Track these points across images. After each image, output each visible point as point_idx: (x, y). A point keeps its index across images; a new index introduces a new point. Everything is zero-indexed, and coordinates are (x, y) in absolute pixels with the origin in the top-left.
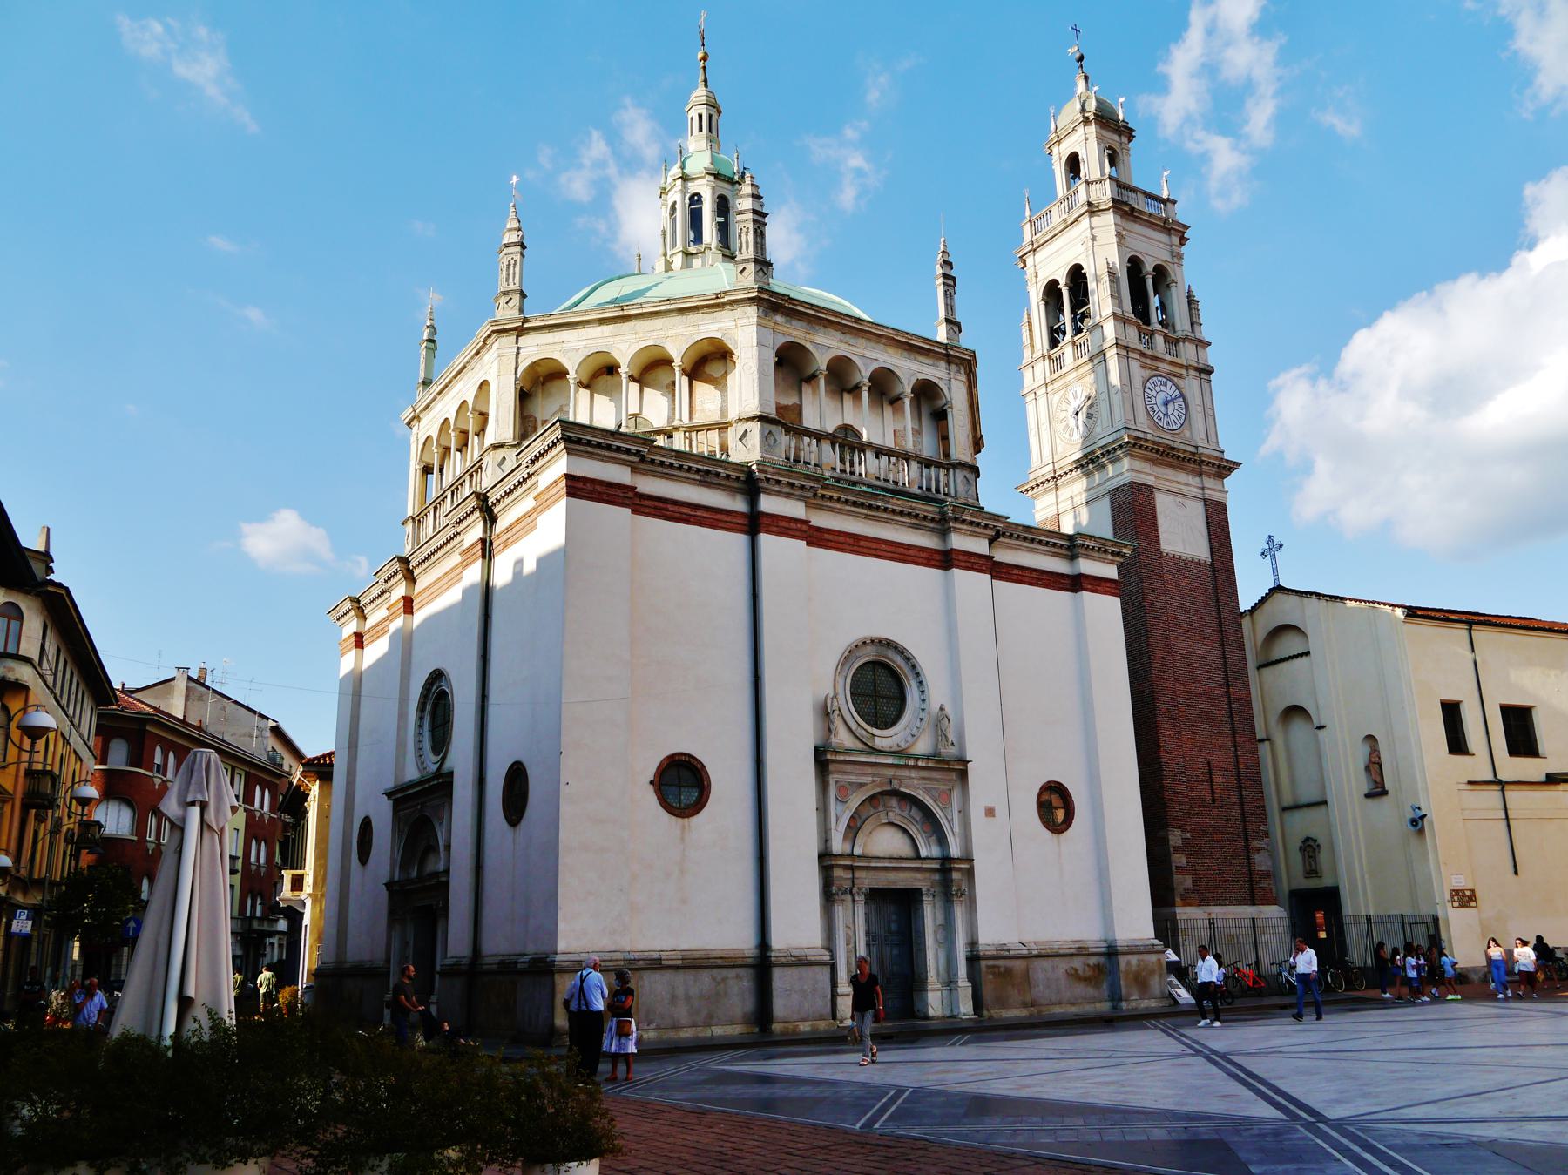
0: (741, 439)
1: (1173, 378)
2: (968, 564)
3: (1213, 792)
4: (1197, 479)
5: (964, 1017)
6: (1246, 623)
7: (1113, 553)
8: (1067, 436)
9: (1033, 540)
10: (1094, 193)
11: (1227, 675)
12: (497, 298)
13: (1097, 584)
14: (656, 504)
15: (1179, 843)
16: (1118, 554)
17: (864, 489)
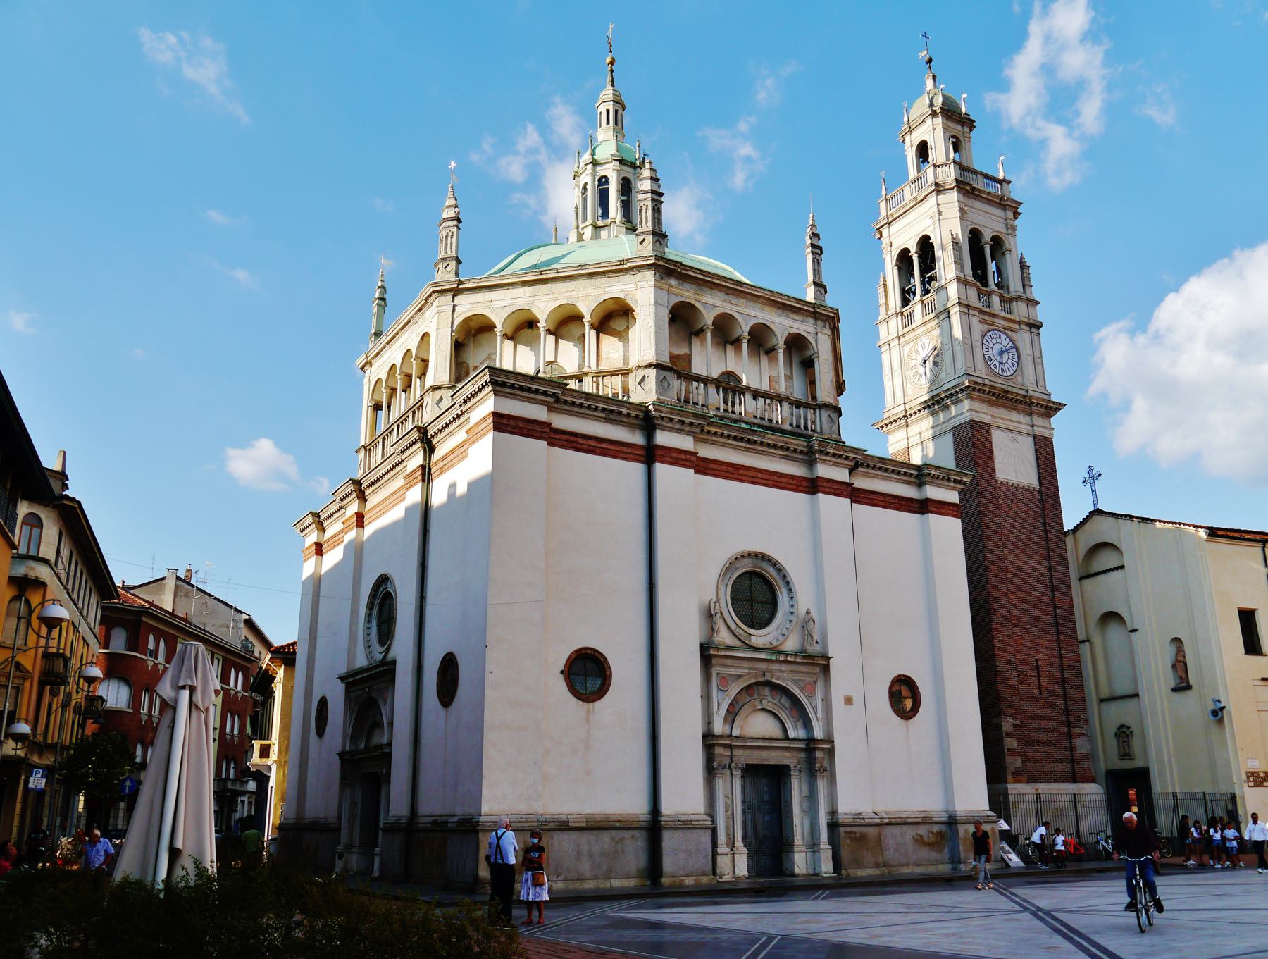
0: (640, 383)
1: (1007, 331)
2: (832, 490)
3: (1040, 685)
4: (1028, 418)
5: (825, 875)
6: (1069, 541)
7: (955, 481)
8: (916, 381)
9: (886, 470)
10: (940, 175)
11: (1052, 585)
12: (436, 264)
13: (941, 508)
14: (569, 437)
15: (1011, 729)
16: (960, 482)
17: (744, 425)
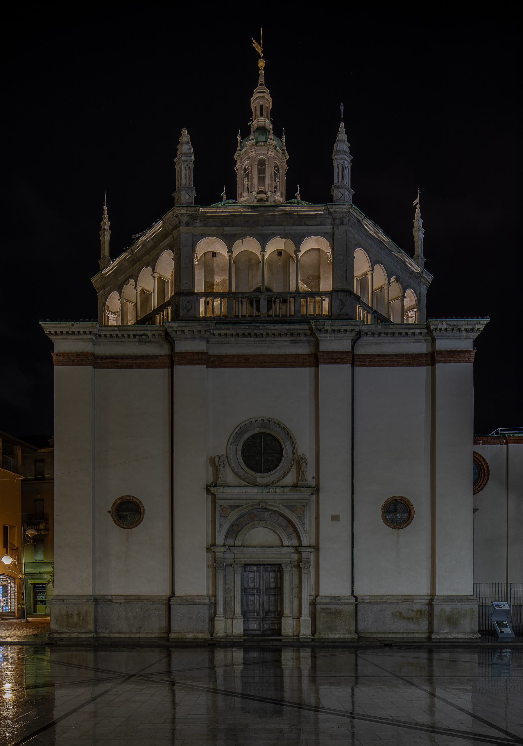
9: (393, 334)
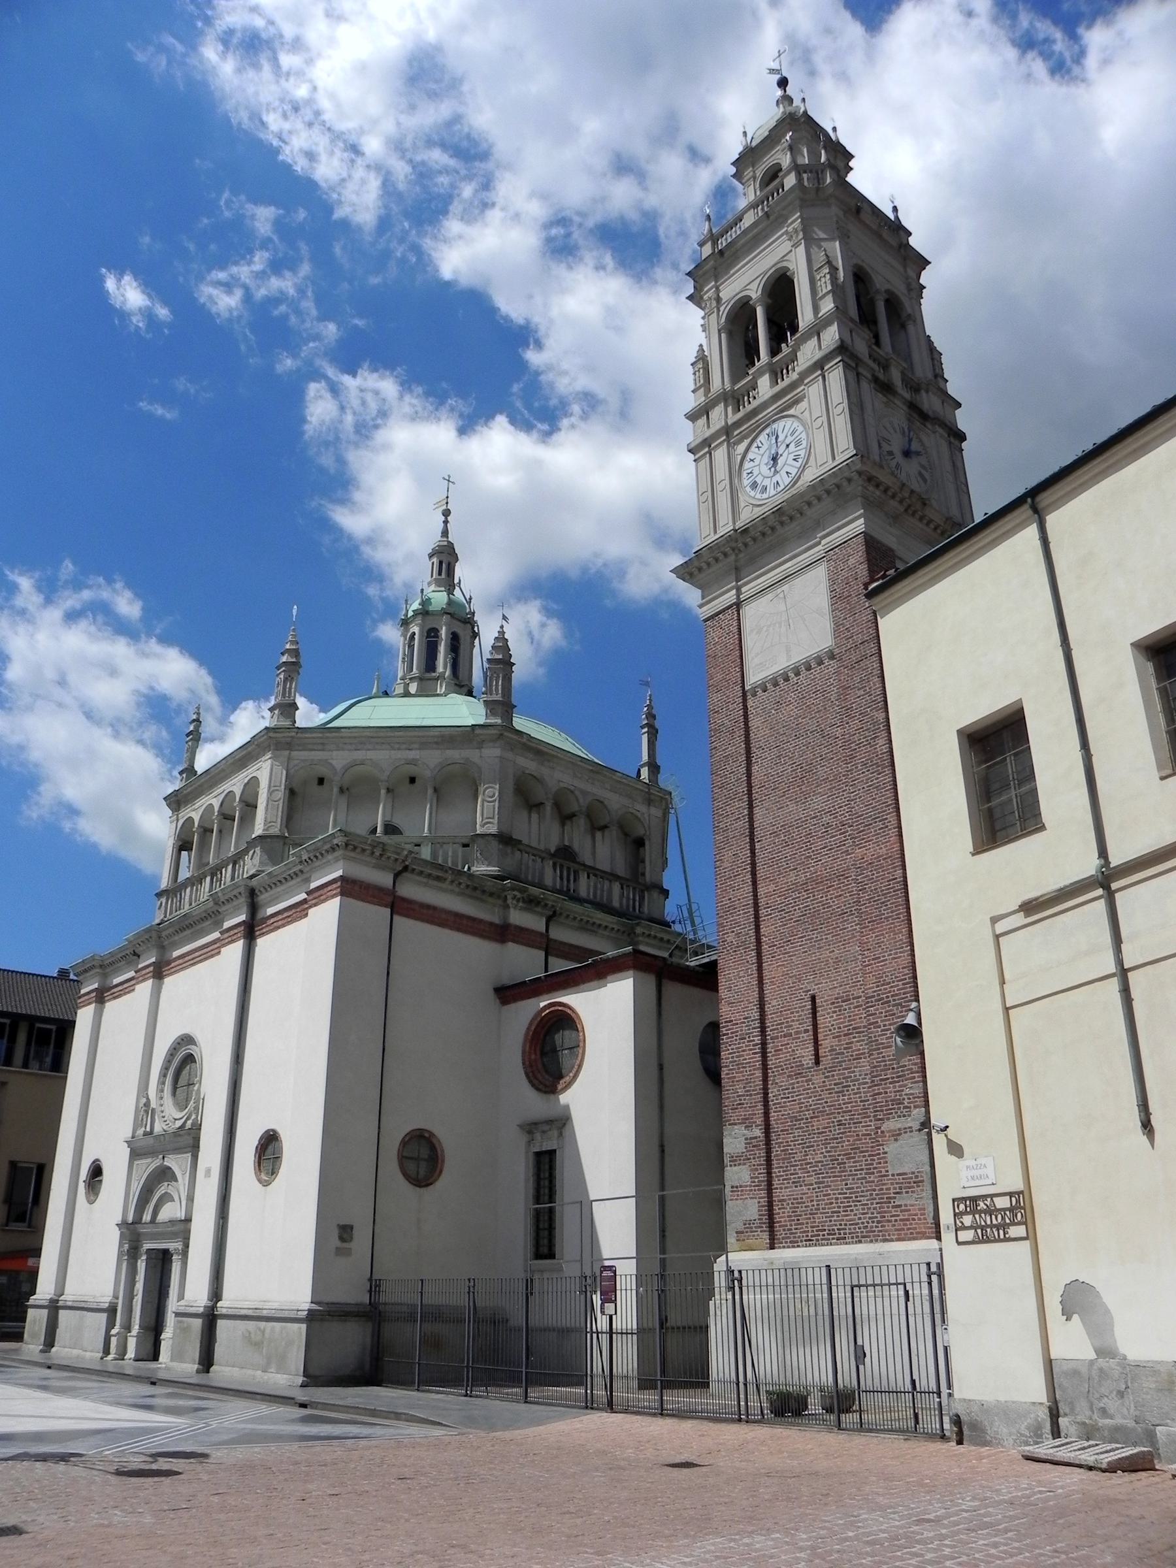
1: (785, 413)
7: (327, 852)
